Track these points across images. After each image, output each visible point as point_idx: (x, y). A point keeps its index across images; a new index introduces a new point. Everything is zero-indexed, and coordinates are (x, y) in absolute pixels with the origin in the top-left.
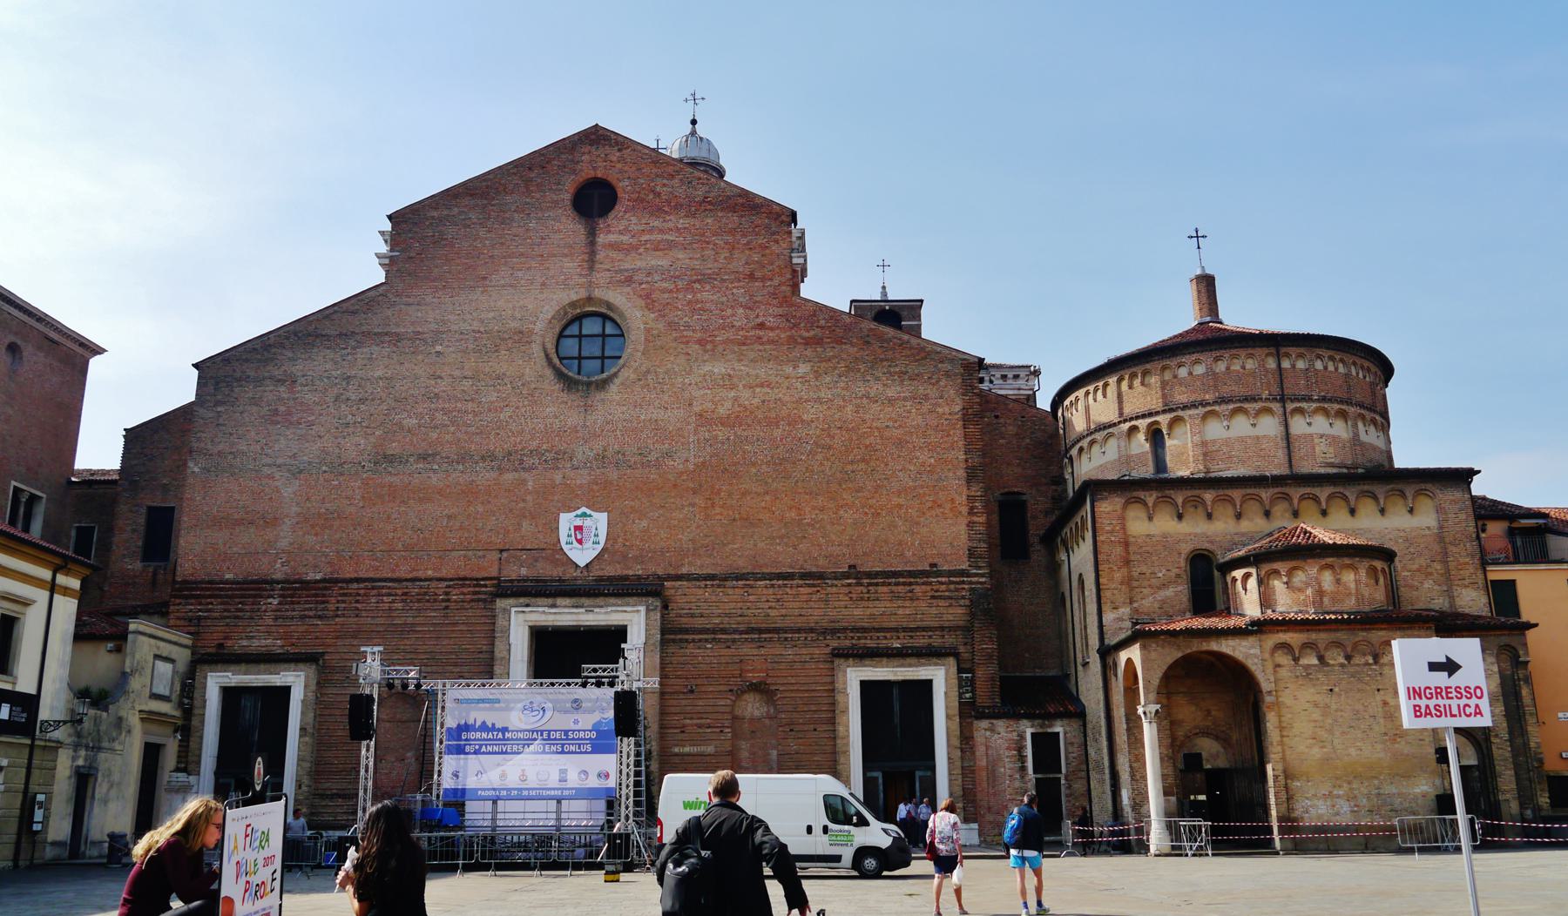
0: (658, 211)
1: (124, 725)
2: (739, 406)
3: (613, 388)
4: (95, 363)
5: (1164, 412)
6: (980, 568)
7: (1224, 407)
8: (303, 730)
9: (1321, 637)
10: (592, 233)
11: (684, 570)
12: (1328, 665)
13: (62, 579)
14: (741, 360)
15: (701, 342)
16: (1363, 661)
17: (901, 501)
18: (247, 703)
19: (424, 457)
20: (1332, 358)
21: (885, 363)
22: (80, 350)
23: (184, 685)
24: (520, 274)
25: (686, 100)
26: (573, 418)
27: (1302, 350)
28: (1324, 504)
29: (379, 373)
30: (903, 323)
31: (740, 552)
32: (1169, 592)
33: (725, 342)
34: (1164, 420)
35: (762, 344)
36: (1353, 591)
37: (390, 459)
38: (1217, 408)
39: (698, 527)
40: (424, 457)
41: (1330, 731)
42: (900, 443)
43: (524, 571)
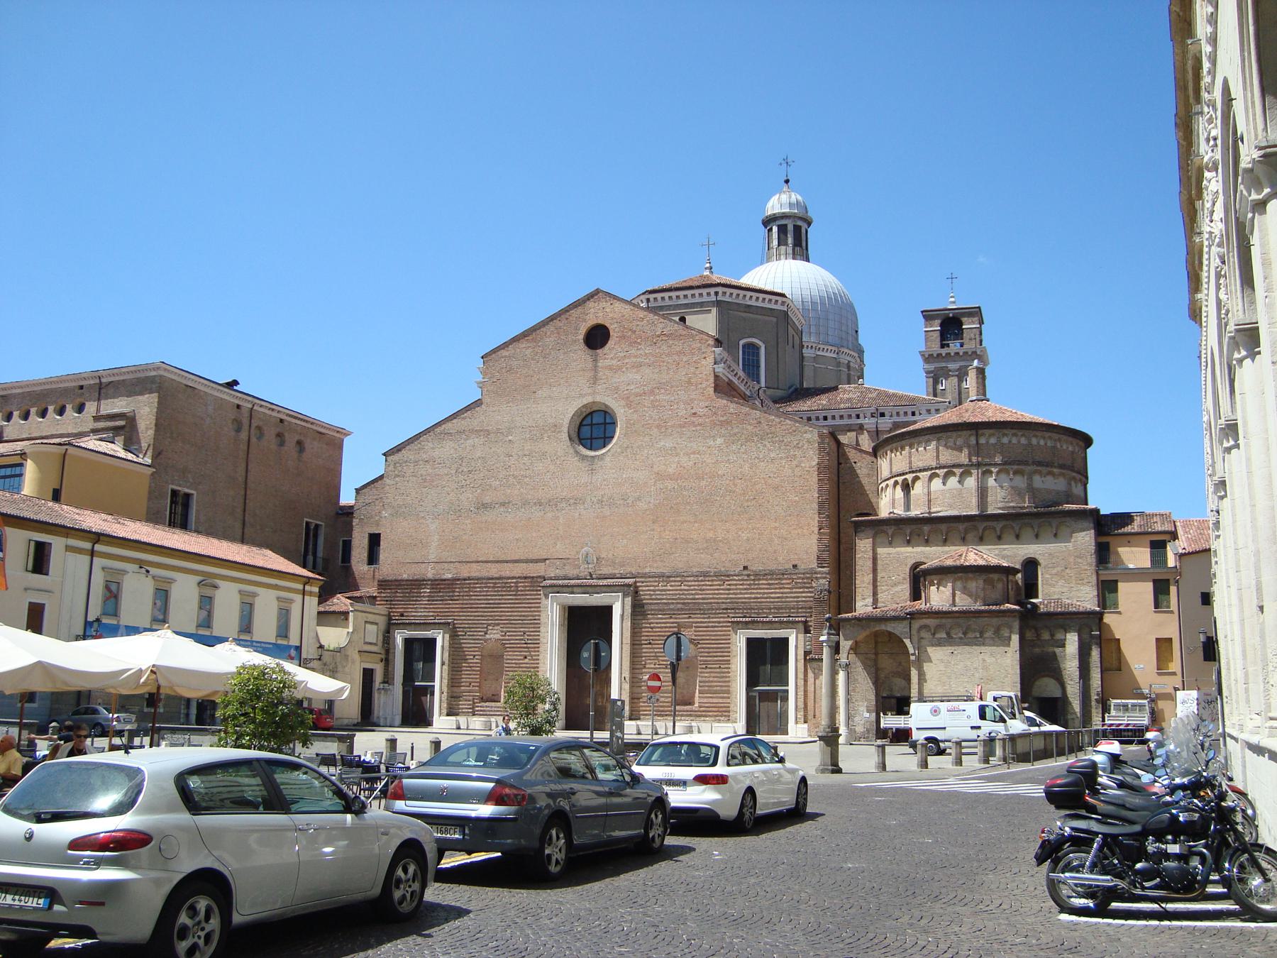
0: (633, 343)
1: (350, 659)
2: (681, 466)
3: (608, 459)
4: (347, 441)
5: (910, 472)
6: (824, 567)
7: (942, 470)
8: (443, 664)
9: (948, 622)
10: (595, 361)
11: (647, 570)
12: (952, 638)
13: (308, 588)
14: (681, 438)
15: (658, 427)
16: (973, 636)
17: (777, 525)
18: (416, 646)
19: (503, 504)
20: (1014, 435)
21: (770, 435)
22: (338, 435)
23: (384, 636)
24: (554, 389)
25: (781, 164)
26: (585, 478)
27: (991, 431)
28: (999, 533)
29: (479, 454)
30: (964, 327)
31: (678, 561)
32: (898, 588)
33: (672, 426)
34: (910, 477)
35: (695, 426)
36: (974, 593)
37: (485, 506)
38: (937, 471)
39: (655, 543)
40: (503, 504)
41: (949, 677)
42: (776, 488)
43: (559, 572)
